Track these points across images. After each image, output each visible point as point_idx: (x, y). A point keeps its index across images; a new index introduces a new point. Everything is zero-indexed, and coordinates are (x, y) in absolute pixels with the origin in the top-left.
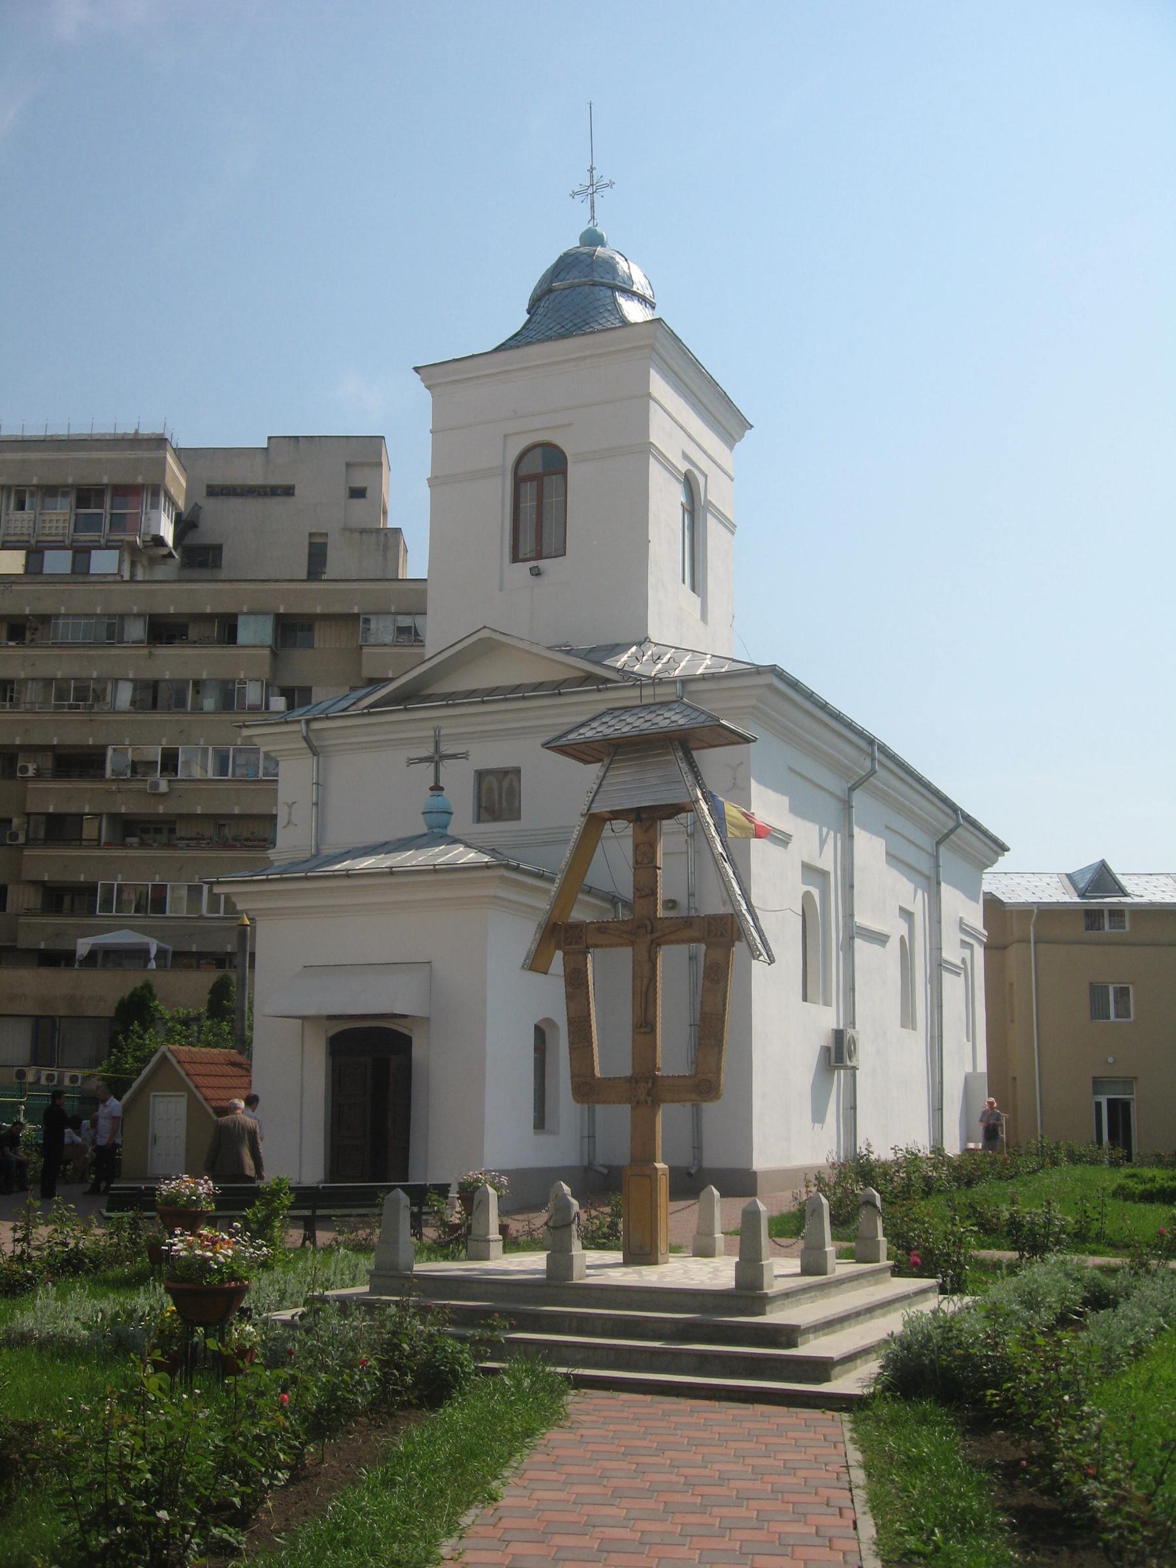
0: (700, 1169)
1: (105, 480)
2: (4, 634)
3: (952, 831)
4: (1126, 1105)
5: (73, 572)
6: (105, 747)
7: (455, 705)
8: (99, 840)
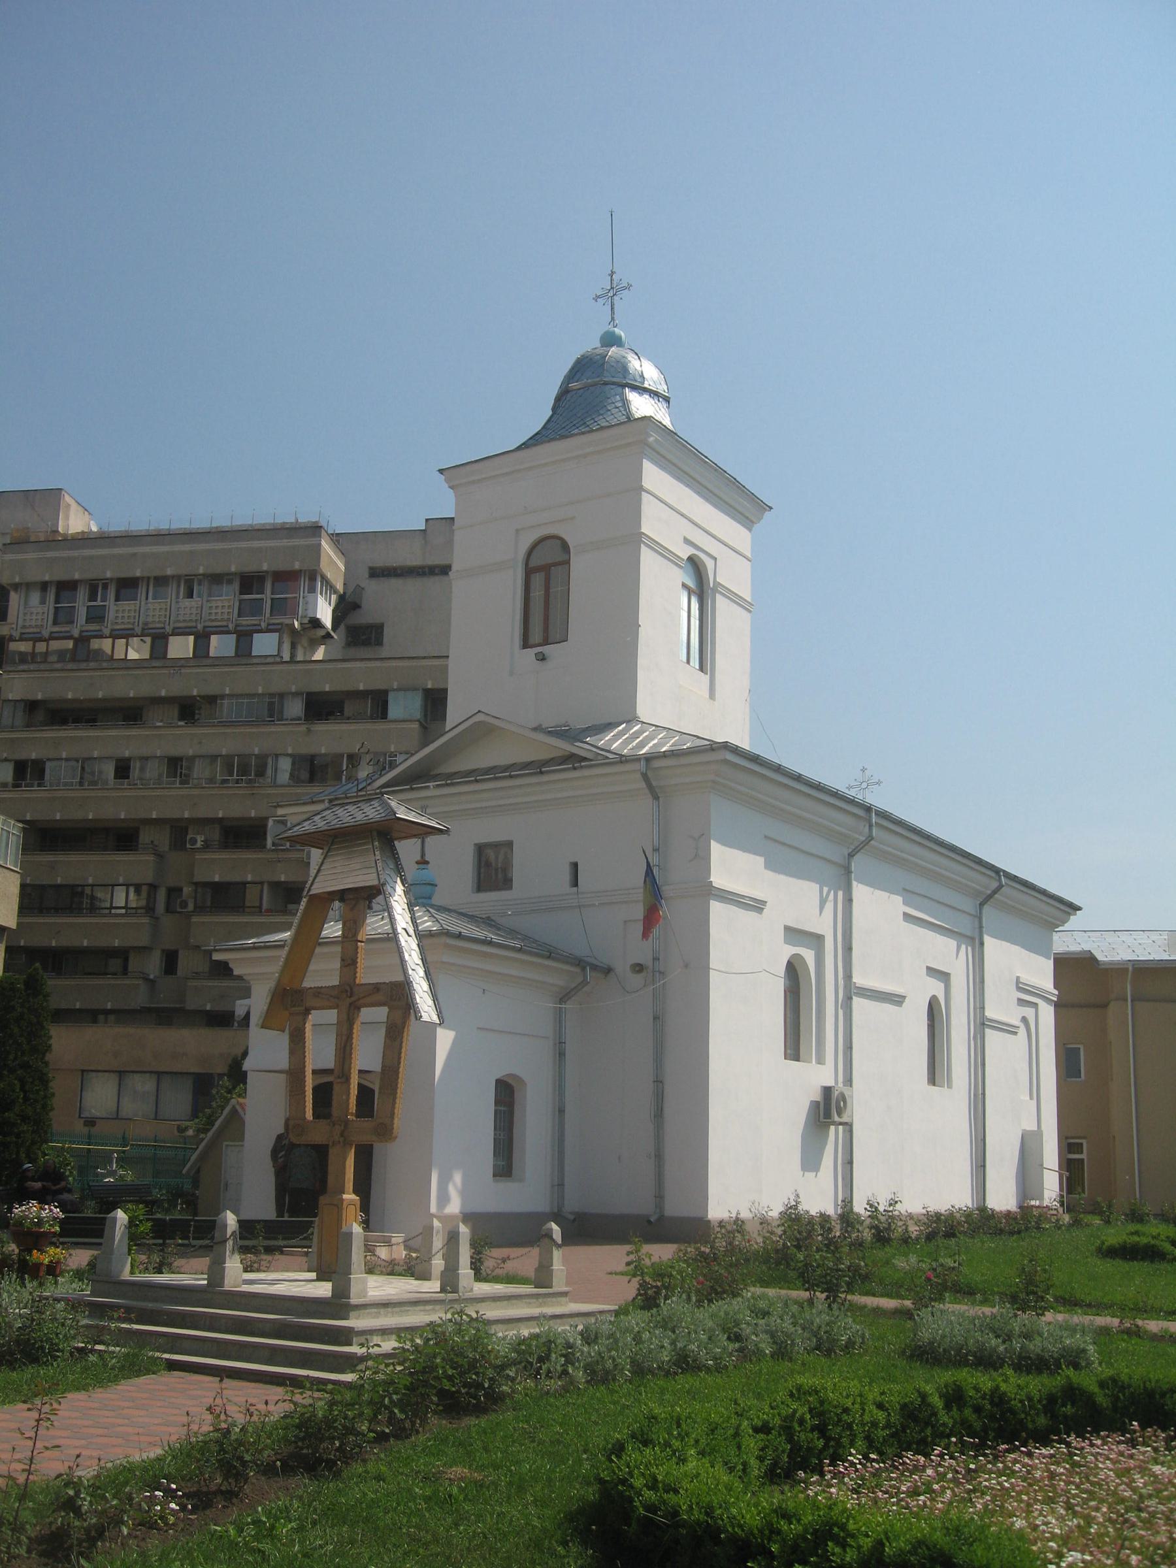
0: (661, 1218)
1: (265, 567)
2: (176, 713)
3: (995, 892)
5: (237, 655)
6: (267, 819)
7: (452, 784)
8: (260, 907)
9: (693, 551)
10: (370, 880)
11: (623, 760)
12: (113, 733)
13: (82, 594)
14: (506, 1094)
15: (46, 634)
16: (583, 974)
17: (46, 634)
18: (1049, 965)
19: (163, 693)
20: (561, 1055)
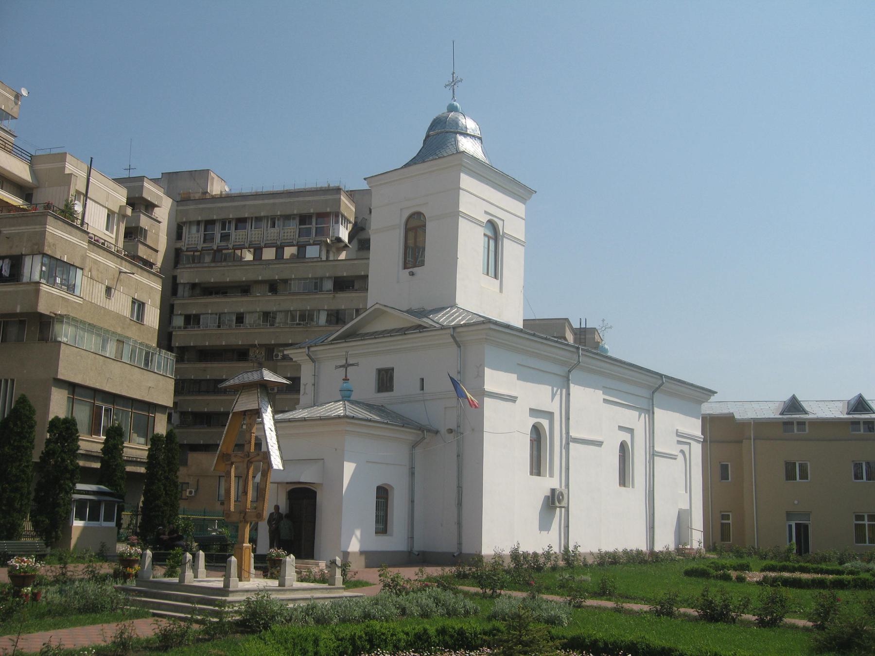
1: (312, 211)
3: (660, 386)
4: (806, 527)
9: (490, 217)
10: (254, 406)
11: (443, 328)
12: (234, 299)
13: (218, 227)
14: (383, 494)
15: (199, 248)
16: (421, 433)
17: (199, 248)
18: (699, 422)
19: (260, 278)
20: (412, 474)
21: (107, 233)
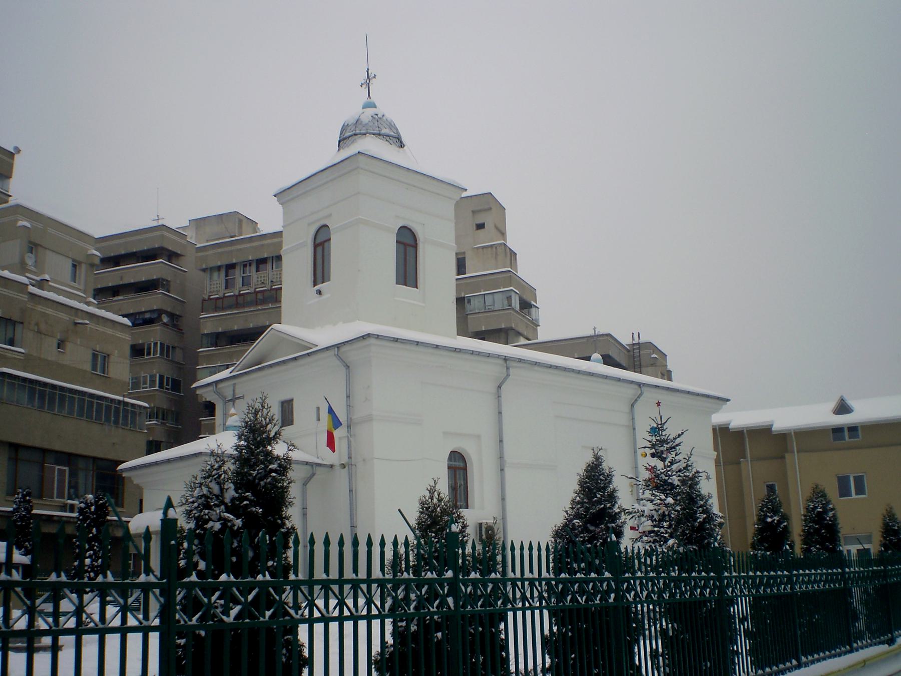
21: (73, 284)
